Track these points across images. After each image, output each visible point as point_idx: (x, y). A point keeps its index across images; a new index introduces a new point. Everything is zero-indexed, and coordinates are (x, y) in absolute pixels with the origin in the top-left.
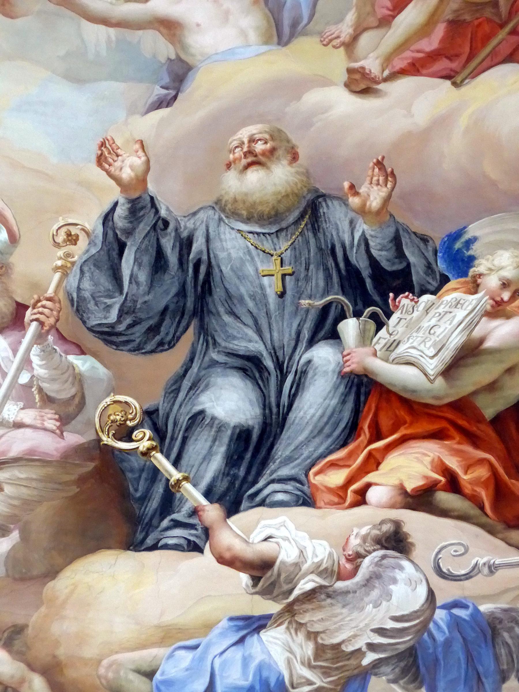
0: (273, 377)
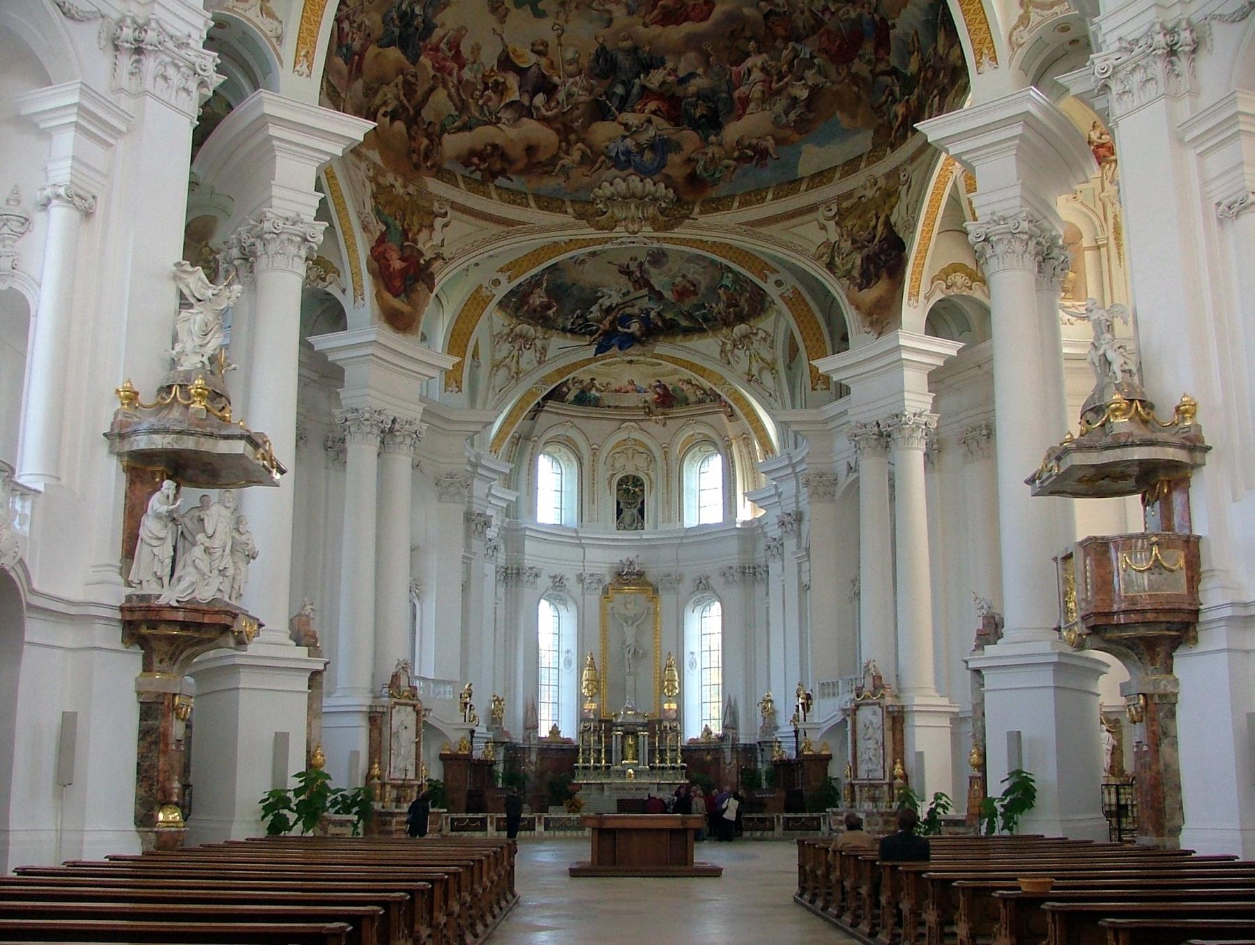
0: (628, 85)
